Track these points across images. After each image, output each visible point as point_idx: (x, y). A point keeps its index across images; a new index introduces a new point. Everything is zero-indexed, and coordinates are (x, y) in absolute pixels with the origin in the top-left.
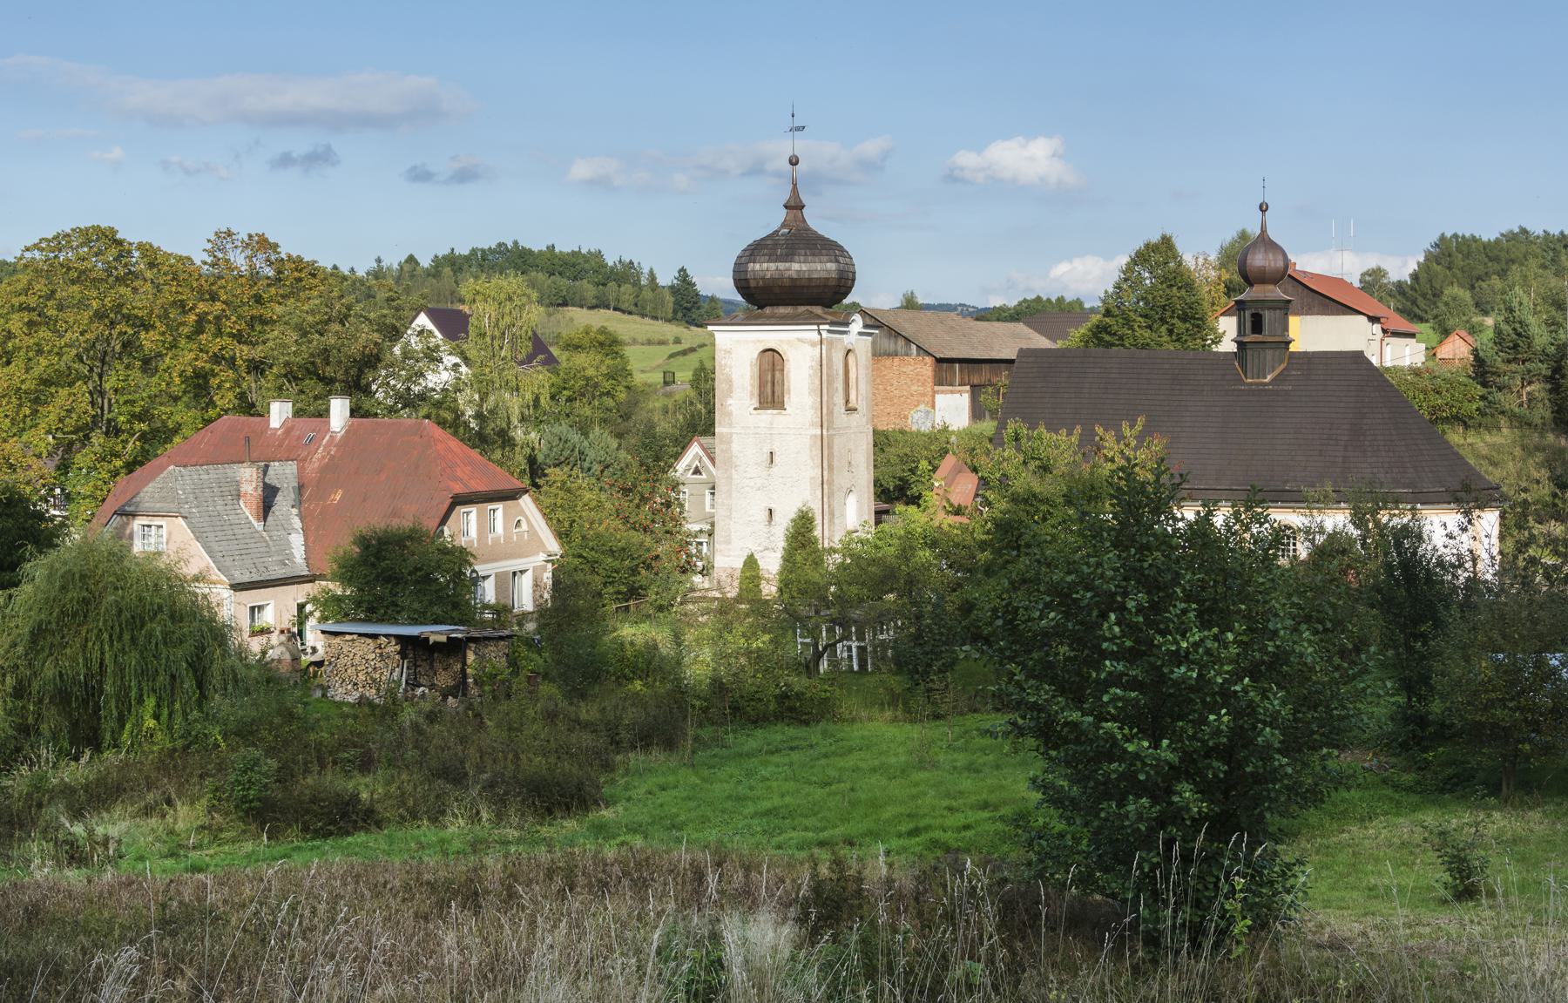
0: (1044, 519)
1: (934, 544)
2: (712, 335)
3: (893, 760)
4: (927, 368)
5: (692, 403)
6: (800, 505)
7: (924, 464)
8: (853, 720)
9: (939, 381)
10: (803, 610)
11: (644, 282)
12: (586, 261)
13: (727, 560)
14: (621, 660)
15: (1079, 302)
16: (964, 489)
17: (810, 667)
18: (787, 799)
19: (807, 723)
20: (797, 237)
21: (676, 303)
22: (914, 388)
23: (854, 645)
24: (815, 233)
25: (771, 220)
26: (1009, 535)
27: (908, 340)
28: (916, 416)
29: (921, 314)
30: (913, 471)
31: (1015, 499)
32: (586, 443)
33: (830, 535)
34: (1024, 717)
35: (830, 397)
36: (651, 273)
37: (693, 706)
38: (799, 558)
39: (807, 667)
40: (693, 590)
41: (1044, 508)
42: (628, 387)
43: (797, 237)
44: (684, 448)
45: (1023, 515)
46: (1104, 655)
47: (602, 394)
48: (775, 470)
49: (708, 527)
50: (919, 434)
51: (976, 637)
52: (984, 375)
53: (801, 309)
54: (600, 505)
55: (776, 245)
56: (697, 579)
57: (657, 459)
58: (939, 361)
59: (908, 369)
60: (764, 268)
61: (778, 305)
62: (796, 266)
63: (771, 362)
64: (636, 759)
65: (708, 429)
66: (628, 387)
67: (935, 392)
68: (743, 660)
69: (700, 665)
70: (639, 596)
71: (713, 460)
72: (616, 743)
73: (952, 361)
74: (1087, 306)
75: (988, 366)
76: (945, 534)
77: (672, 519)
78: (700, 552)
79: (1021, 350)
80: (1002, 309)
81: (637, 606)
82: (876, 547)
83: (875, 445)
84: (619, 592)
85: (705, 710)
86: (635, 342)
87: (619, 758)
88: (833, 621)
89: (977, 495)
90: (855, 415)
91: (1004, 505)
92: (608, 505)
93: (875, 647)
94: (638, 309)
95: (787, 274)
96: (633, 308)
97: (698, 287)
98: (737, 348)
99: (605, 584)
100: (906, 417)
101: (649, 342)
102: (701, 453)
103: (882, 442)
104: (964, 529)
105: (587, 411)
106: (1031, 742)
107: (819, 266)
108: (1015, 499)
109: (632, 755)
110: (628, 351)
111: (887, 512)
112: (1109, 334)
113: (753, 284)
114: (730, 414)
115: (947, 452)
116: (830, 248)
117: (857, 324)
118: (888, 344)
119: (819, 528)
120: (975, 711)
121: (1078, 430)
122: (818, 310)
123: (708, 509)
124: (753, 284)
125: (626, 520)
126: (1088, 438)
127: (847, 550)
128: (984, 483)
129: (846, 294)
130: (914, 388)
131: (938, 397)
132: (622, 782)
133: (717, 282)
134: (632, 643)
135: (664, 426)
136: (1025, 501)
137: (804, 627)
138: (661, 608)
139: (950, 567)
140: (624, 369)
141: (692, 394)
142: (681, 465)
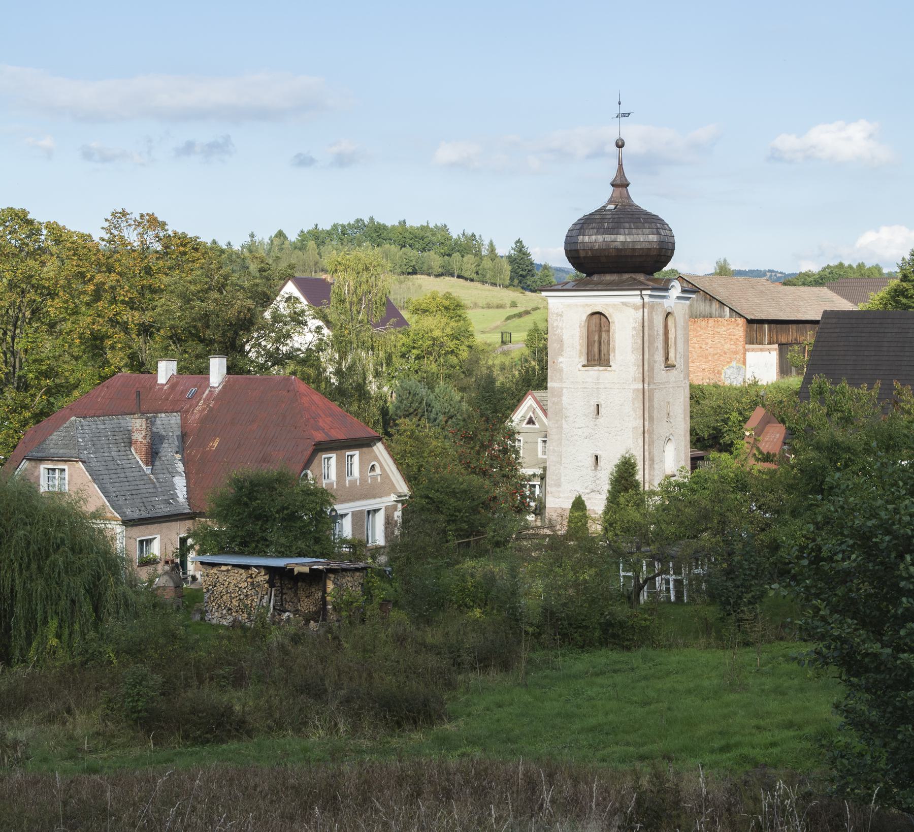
0: (846, 466)
2: (545, 299)
3: (706, 683)
4: (739, 328)
5: (526, 361)
6: (623, 452)
7: (735, 416)
9: (752, 340)
10: (625, 546)
11: (484, 252)
12: (434, 235)
13: (558, 502)
14: (462, 590)
15: (878, 268)
16: (773, 439)
17: (631, 598)
18: (611, 717)
19: (628, 649)
20: (623, 213)
22: (727, 346)
23: (671, 578)
24: (638, 208)
25: (599, 197)
28: (729, 372)
29: (734, 280)
30: (725, 421)
32: (432, 396)
33: (650, 479)
35: (651, 355)
36: (491, 244)
37: (527, 633)
38: (622, 500)
39: (629, 598)
40: (527, 527)
41: (846, 456)
42: (470, 347)
43: (623, 213)
46: (902, 592)
47: (447, 353)
48: (601, 420)
49: (539, 472)
50: (731, 388)
51: (783, 572)
52: (792, 334)
53: (626, 276)
56: (531, 518)
58: (750, 322)
59: (722, 329)
60: (593, 239)
62: (621, 238)
63: (599, 323)
64: (475, 678)
65: (542, 384)
66: (470, 347)
67: (746, 350)
68: (571, 592)
70: (479, 533)
71: (545, 412)
72: (458, 665)
73: (761, 322)
74: (885, 271)
75: (794, 326)
76: (756, 478)
78: (533, 493)
79: (825, 312)
80: (807, 275)
82: (693, 490)
83: (691, 398)
84: (462, 530)
85: (537, 636)
86: (476, 305)
87: (460, 677)
88: (653, 557)
90: (674, 372)
93: (690, 581)
94: (479, 277)
96: (474, 276)
100: (719, 373)
101: (489, 306)
102: (535, 405)
103: (697, 396)
104: (772, 473)
105: (434, 367)
107: (642, 238)
108: (818, 447)
109: (471, 675)
110: (470, 314)
111: (701, 458)
112: (906, 297)
113: (582, 254)
114: (561, 370)
115: (756, 405)
117: (676, 290)
118: (703, 307)
119: (640, 473)
120: (782, 639)
121: (878, 384)
122: (641, 277)
123: (540, 455)
124: (582, 254)
125: (467, 465)
126: (887, 390)
128: (791, 432)
129: (665, 263)
130: (727, 346)
132: (463, 699)
136: (829, 449)
137: (626, 562)
138: (497, 544)
139: (760, 508)
140: (466, 330)
141: (527, 352)
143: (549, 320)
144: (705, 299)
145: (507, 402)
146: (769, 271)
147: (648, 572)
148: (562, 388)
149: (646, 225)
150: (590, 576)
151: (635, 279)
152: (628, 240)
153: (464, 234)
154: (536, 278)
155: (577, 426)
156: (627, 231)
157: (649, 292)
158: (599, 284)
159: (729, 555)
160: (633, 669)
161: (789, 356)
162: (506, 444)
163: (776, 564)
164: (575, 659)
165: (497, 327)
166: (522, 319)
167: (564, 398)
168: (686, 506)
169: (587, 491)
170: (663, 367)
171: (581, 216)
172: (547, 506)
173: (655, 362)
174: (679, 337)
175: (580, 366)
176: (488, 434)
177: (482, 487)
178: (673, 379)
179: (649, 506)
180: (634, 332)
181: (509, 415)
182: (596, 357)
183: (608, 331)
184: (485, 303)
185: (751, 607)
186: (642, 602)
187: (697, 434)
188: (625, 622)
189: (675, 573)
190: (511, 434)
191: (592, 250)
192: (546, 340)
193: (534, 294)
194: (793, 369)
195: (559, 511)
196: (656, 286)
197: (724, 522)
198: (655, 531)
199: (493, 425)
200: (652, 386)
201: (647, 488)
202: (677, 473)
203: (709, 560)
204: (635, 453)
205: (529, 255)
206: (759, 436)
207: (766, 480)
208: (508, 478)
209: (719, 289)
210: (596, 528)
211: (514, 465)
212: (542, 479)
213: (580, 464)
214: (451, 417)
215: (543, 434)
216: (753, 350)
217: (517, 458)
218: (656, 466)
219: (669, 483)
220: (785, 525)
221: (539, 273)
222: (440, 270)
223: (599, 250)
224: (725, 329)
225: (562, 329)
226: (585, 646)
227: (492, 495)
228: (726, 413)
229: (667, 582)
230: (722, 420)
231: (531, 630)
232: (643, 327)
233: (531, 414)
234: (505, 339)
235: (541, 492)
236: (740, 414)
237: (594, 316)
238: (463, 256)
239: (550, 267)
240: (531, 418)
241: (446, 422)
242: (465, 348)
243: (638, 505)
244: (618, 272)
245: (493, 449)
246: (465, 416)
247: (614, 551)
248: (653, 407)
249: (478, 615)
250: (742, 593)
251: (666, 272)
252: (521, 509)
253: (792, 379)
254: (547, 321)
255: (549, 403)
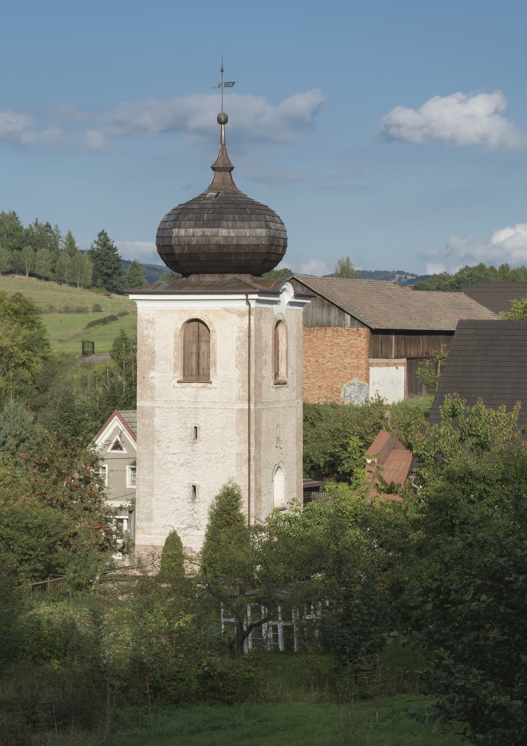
0: (481, 498)
1: (364, 523)
2: (133, 303)
4: (361, 340)
5: (112, 375)
6: (225, 482)
7: (355, 442)
8: (278, 700)
10: (227, 590)
11: (62, 246)
13: (149, 538)
16: (397, 466)
17: (233, 647)
19: (230, 703)
21: (97, 269)
22: (348, 360)
23: (280, 625)
24: (244, 197)
25: (199, 182)
26: (442, 516)
27: (342, 310)
28: (349, 390)
29: (357, 283)
30: (344, 447)
31: (450, 478)
33: (256, 512)
34: (452, 701)
35: (259, 370)
38: (223, 537)
39: (231, 647)
40: (112, 568)
41: (480, 486)
42: (43, 358)
44: (104, 422)
45: (458, 494)
47: (17, 365)
48: (199, 445)
50: (351, 408)
52: (423, 346)
53: (229, 277)
54: (15, 481)
55: (202, 209)
56: (117, 557)
57: (76, 433)
58: (375, 332)
59: (342, 340)
60: (188, 233)
61: (204, 273)
62: (223, 232)
63: (197, 331)
65: (129, 402)
66: (43, 358)
67: (369, 365)
68: (164, 640)
69: (119, 644)
70: (56, 574)
71: (134, 435)
73: (388, 332)
75: (425, 337)
76: (377, 512)
77: (91, 496)
78: (120, 529)
79: (461, 322)
80: (442, 277)
81: (54, 584)
82: (305, 526)
83: (305, 420)
84: (35, 570)
85: (125, 690)
86: (51, 309)
87: (36, 737)
88: (259, 601)
89: (411, 473)
90: (285, 390)
91: (440, 484)
92: (23, 481)
93: (301, 628)
94: (55, 275)
95: (213, 241)
96: (49, 274)
97: (120, 252)
98: (160, 318)
99: (21, 562)
100: (338, 391)
101: (67, 310)
102: (122, 427)
103: (312, 416)
104: (397, 507)
106: (458, 725)
107: (248, 232)
108: (450, 478)
109: (49, 734)
110: (45, 320)
111: (316, 489)
113: (177, 250)
114: (152, 387)
115: (380, 428)
116: (260, 213)
117: (288, 294)
118: (320, 314)
119: (246, 505)
120: (404, 691)
121: (518, 405)
122: (247, 278)
123: (128, 485)
125: (43, 496)
127: (273, 527)
128: (419, 459)
130: (348, 360)
131: (374, 372)
133: (139, 247)
134: (49, 622)
135: (82, 399)
136: (461, 479)
137: (228, 606)
138: (79, 587)
139: (381, 546)
141: (113, 365)
142: (101, 440)
143: (138, 327)
144: (323, 305)
145: (89, 424)
146: (399, 272)
147: (253, 618)
148: (153, 408)
149: (254, 217)
150: (186, 622)
151: (240, 281)
152: (232, 234)
153: (36, 224)
154: (123, 277)
155: (172, 451)
156: (230, 224)
157: (256, 296)
158: (198, 285)
159: (346, 598)
160: (234, 726)
161: (418, 373)
162: (89, 472)
163: (399, 609)
164: (169, 715)
165: (77, 335)
166: (107, 326)
167: (156, 419)
168: (296, 544)
169: (183, 526)
170: (272, 384)
171: (175, 205)
172: (137, 543)
173: (263, 378)
174: (291, 349)
175: (174, 382)
176: (66, 460)
177: (59, 522)
178: (284, 398)
179: (254, 544)
180: (239, 343)
181: (91, 438)
182: (194, 372)
183: (208, 342)
184: (62, 306)
185: (369, 656)
186: (246, 651)
187: (311, 462)
188: (226, 674)
189: (283, 619)
190: (95, 461)
191: (188, 245)
192: (135, 351)
193: (120, 297)
194: (424, 387)
195: (150, 549)
196: (265, 289)
197: (340, 562)
198: (261, 572)
199: (73, 449)
200: (259, 406)
201: (252, 523)
202: (288, 506)
203: (323, 604)
204: (239, 483)
205: (115, 250)
206: (383, 464)
207: (389, 513)
208: (90, 511)
209: (339, 293)
210: (192, 568)
211: (97, 497)
212: (130, 512)
213: (175, 496)
214: (23, 441)
215: (131, 461)
216: (377, 365)
217: (100, 489)
218: (263, 498)
219: (279, 518)
220: (410, 565)
221: (127, 271)
222: (9, 267)
223: (199, 246)
224: (344, 339)
225: (153, 338)
226: (181, 700)
227: (72, 531)
228: (346, 437)
229: (275, 629)
230: (341, 446)
231: (117, 683)
232: (249, 337)
233: (117, 437)
234: (86, 350)
235: (129, 527)
236: (362, 438)
237: (192, 324)
238: (35, 250)
239: (141, 265)
240: (117, 442)
241: (17, 446)
242: (39, 360)
243: (242, 542)
244: (220, 273)
245: (73, 478)
246: (39, 439)
247: (214, 595)
248: (260, 430)
249: (56, 668)
250: (360, 640)
251: (278, 273)
252: (107, 547)
253: (422, 398)
254: (136, 328)
255: (138, 425)
